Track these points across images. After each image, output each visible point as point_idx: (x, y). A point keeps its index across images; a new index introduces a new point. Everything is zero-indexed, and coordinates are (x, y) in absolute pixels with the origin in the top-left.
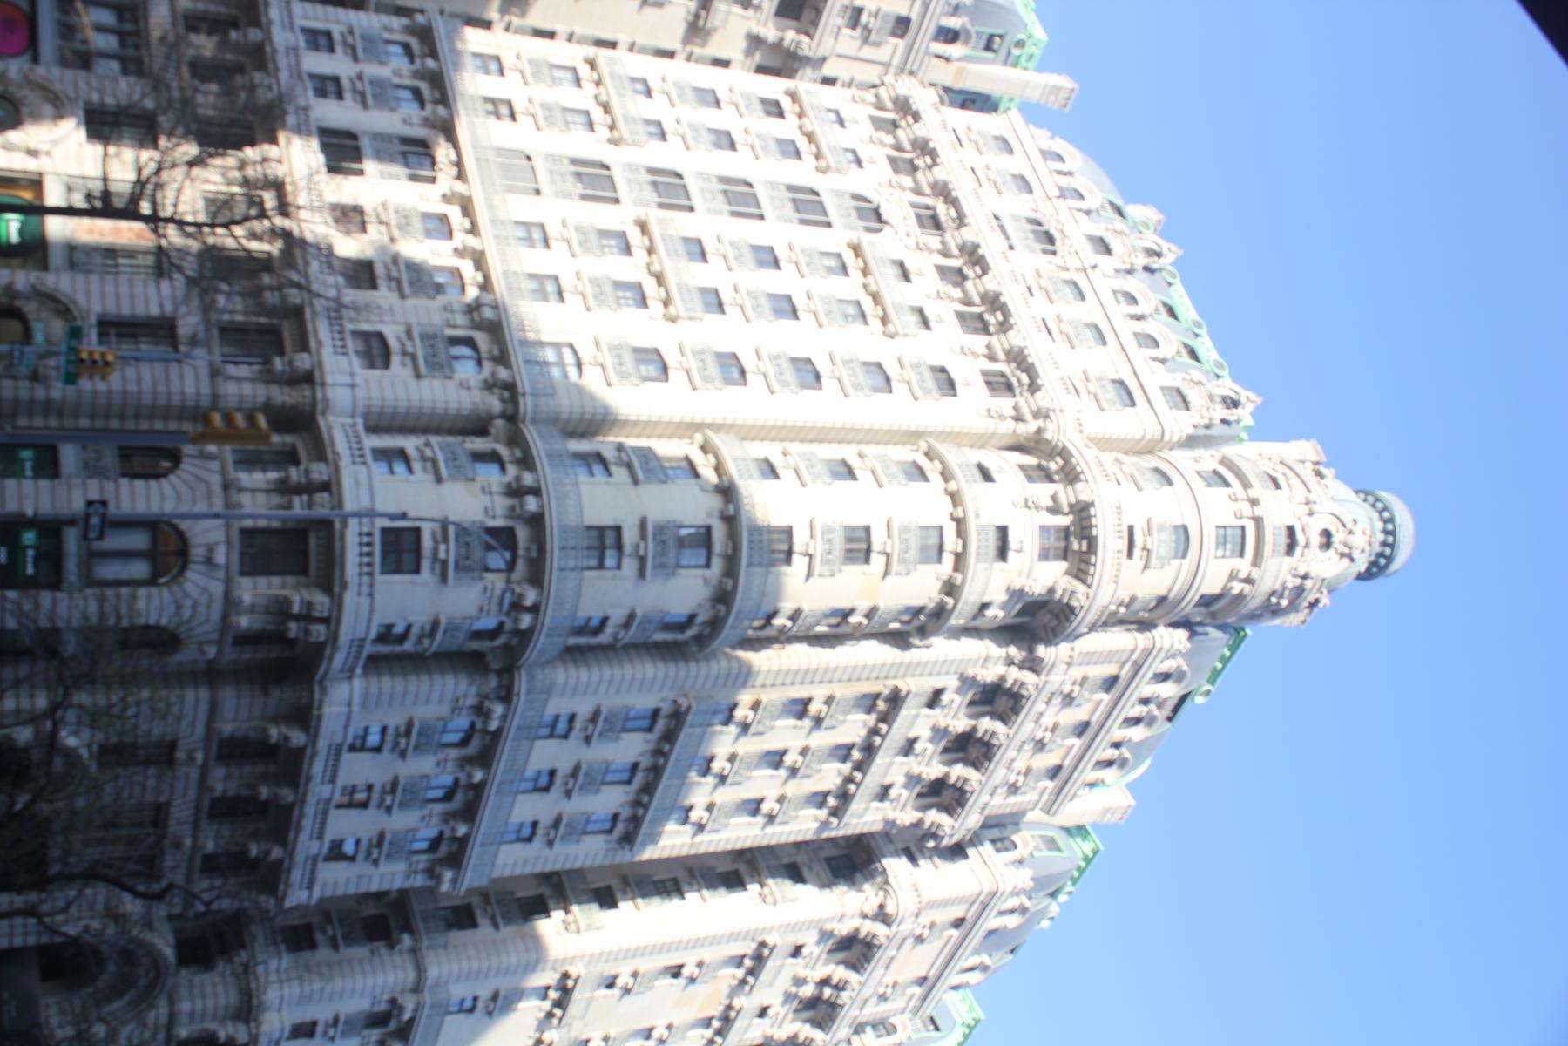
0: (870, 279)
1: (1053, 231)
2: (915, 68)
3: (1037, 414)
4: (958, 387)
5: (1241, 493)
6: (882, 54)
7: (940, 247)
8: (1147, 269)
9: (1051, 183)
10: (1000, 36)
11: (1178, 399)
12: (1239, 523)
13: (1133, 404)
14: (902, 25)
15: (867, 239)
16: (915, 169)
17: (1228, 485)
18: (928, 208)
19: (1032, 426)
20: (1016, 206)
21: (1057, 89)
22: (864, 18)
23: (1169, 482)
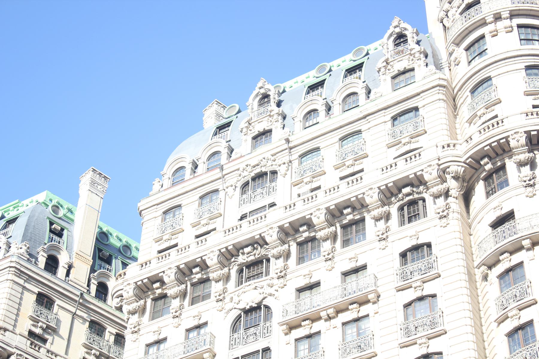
0: (323, 314)
1: (253, 174)
2: (78, 293)
3: (444, 181)
4: (420, 242)
5: (491, 27)
6: (65, 318)
8: (279, 104)
9: (204, 176)
10: (51, 224)
11: (402, 78)
12: (515, 29)
13: (416, 109)
14: (44, 301)
15: (277, 317)
16: (164, 296)
17: (483, 37)
18: (241, 271)
19: (453, 185)
20: (232, 205)
21: (93, 183)
22: (38, 331)
23: (489, 79)
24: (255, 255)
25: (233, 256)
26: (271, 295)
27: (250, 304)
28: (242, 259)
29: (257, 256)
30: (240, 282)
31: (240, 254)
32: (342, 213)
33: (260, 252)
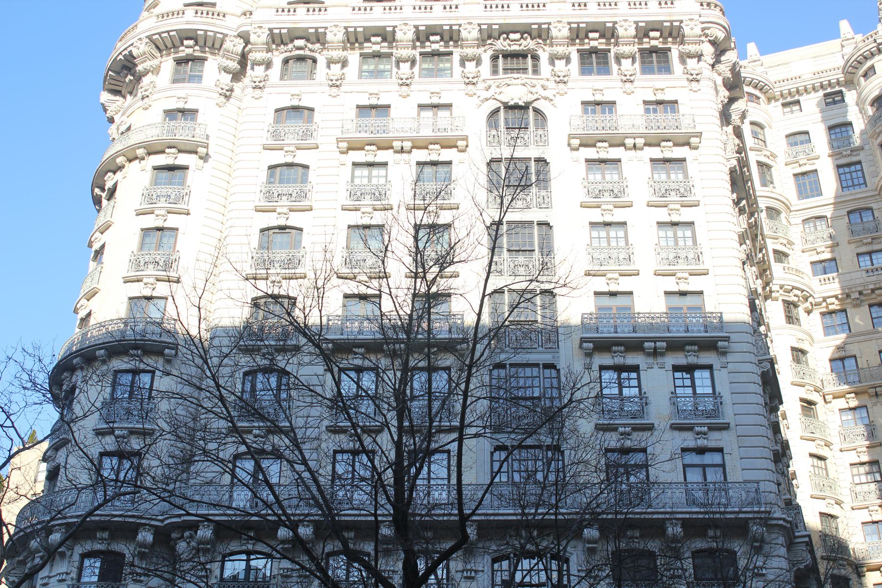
7: (263, 67)
18: (495, 58)
24: (520, 45)
25: (490, 37)
26: (546, 98)
27: (516, 101)
28: (501, 44)
29: (522, 47)
30: (495, 71)
31: (501, 38)
32: (646, 35)
33: (528, 44)
